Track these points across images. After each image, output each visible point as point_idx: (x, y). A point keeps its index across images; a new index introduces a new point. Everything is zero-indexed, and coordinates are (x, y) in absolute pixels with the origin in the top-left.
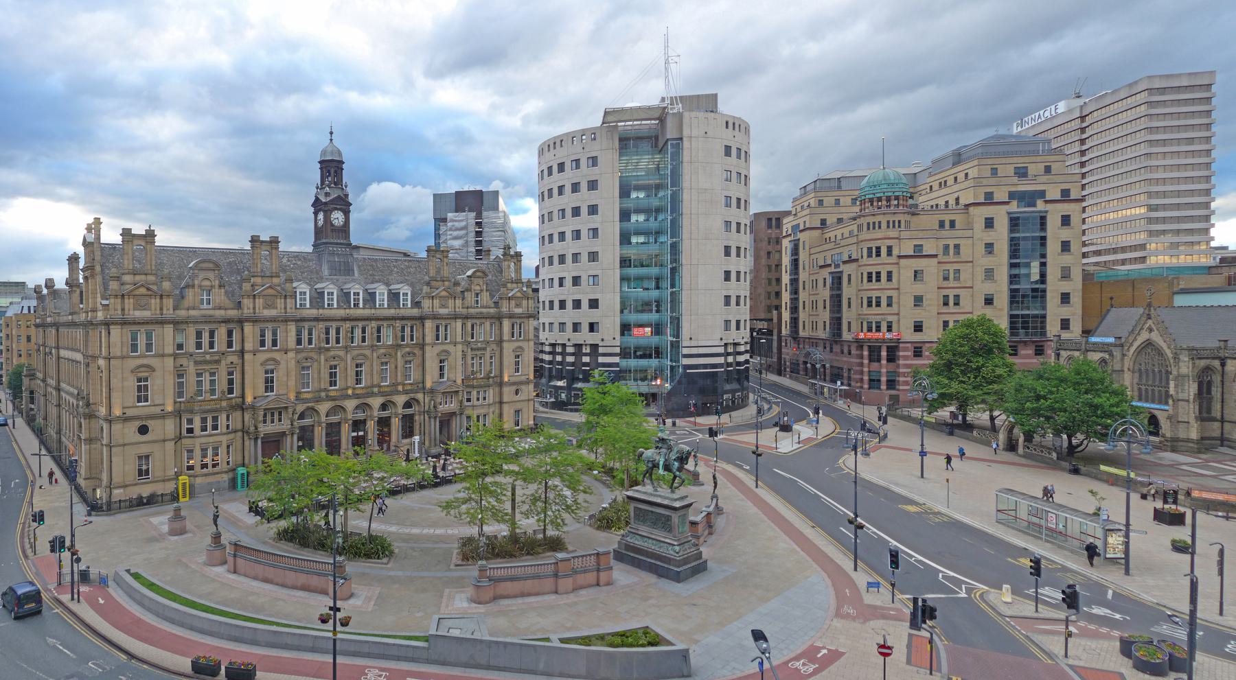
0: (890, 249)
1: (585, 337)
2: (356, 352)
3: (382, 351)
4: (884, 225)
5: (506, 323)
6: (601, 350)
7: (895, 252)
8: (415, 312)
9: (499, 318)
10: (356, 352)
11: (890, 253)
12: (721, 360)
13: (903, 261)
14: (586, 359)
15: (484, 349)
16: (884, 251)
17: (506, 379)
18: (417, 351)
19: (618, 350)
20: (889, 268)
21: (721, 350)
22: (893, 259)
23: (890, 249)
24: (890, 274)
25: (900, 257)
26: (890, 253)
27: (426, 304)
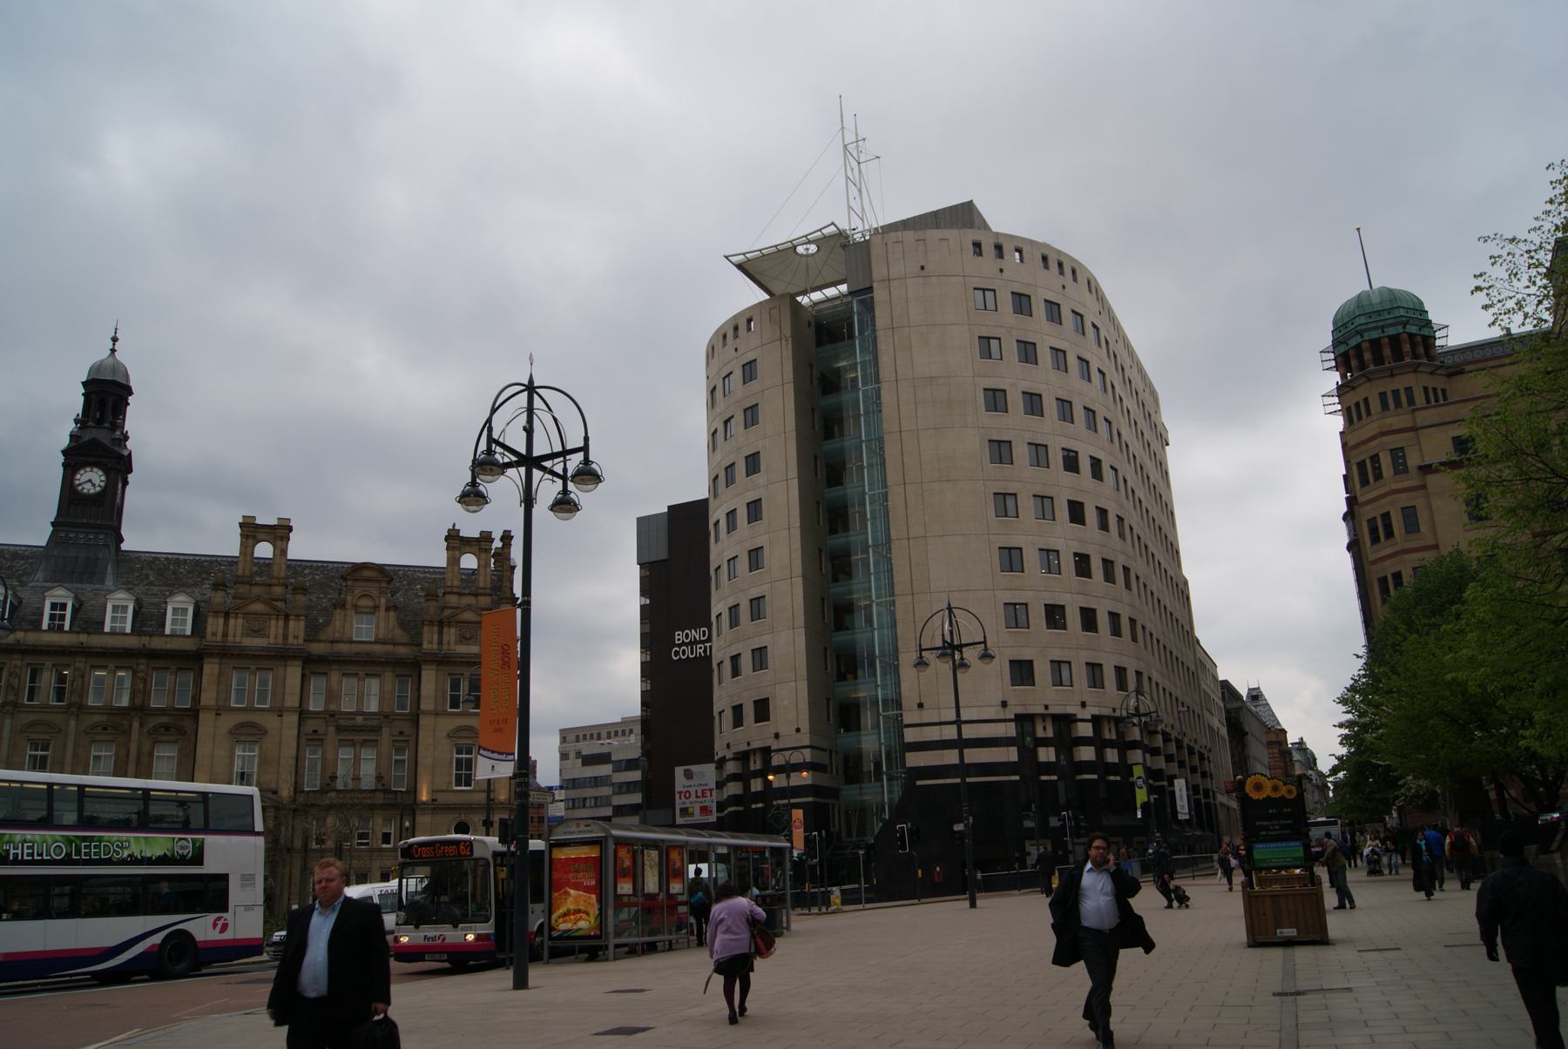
0: (1398, 455)
1: (754, 734)
2: (32, 717)
3: (97, 718)
4: (1375, 405)
5: (429, 677)
6: (777, 760)
7: (1413, 461)
8: (190, 645)
9: (410, 668)
10: (32, 717)
11: (1400, 467)
12: (1012, 754)
13: (1432, 480)
14: (756, 785)
15: (377, 730)
16: (1386, 461)
17: (424, 796)
18: (187, 724)
19: (807, 755)
20: (1405, 500)
21: (1010, 730)
22: (1412, 480)
23: (1398, 455)
24: (1410, 514)
25: (1426, 469)
26: (1400, 467)
27: (214, 625)
